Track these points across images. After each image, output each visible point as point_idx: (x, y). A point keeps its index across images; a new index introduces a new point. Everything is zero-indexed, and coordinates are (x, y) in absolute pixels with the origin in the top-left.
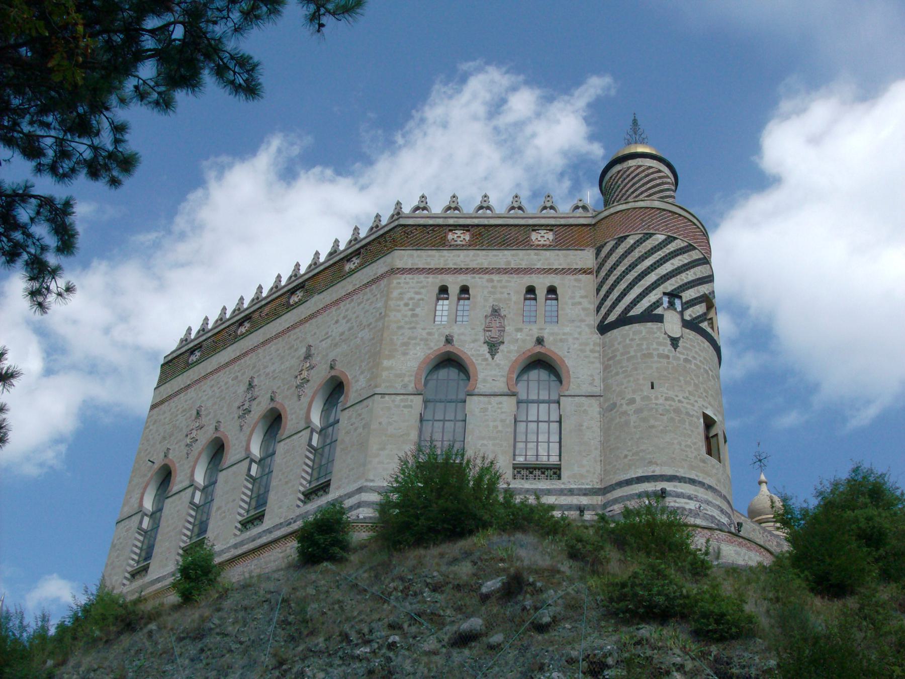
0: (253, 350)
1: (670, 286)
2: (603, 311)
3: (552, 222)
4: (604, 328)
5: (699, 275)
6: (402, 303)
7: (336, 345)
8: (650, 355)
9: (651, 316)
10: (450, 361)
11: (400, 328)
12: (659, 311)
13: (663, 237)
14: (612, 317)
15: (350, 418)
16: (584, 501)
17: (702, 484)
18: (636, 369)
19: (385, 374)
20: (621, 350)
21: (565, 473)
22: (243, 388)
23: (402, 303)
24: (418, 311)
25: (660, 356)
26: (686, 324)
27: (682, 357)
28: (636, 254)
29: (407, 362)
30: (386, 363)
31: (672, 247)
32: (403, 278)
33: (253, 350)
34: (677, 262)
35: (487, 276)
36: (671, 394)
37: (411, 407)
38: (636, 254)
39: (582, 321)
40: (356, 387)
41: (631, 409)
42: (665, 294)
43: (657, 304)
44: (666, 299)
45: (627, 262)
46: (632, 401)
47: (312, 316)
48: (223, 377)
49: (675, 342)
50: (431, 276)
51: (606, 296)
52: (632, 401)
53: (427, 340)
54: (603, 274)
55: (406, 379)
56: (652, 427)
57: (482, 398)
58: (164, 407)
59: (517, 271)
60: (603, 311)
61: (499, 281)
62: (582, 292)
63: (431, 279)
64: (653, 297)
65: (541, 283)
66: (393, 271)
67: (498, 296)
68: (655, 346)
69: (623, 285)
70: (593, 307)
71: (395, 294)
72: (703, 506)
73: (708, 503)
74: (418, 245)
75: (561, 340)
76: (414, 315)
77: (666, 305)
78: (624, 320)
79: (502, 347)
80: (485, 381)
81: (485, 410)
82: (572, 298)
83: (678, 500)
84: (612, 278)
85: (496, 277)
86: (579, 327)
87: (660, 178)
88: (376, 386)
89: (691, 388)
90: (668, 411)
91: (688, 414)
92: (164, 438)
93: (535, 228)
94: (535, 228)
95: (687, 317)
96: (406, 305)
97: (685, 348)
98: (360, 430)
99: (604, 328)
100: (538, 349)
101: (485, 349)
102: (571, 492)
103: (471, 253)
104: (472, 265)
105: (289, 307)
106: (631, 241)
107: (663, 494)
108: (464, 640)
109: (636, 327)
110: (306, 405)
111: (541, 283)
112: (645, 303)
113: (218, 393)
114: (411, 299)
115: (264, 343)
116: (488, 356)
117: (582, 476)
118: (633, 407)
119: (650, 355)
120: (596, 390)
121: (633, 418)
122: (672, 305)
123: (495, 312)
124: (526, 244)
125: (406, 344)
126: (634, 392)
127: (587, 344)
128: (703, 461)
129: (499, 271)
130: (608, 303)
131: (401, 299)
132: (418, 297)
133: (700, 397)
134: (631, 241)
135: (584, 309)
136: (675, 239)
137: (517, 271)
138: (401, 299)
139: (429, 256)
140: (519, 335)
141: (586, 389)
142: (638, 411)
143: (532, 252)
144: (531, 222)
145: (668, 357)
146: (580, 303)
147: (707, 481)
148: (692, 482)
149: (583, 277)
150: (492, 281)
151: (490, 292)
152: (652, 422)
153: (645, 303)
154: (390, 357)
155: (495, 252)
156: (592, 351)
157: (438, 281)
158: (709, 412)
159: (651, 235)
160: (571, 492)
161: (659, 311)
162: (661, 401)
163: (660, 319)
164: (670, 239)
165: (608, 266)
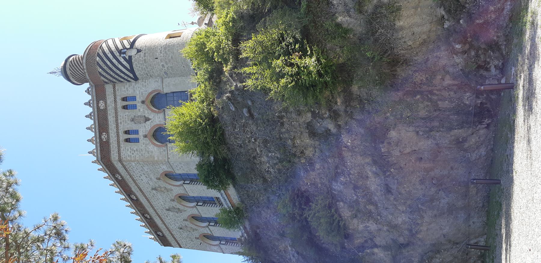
0: (155, 211)
1: (117, 54)
2: (129, 79)
3: (95, 102)
4: (136, 79)
7: (151, 179)
8: (145, 60)
9: (129, 60)
11: (142, 155)
12: (127, 57)
14: (131, 75)
15: (178, 170)
18: (150, 65)
19: (160, 158)
20: (144, 71)
22: (171, 213)
24: (135, 149)
25: (145, 57)
28: (105, 68)
29: (154, 150)
30: (156, 159)
32: (123, 156)
33: (155, 211)
36: (159, 51)
38: (105, 68)
40: (165, 168)
41: (166, 66)
43: (124, 58)
44: (122, 55)
45: (109, 71)
46: (163, 66)
47: (140, 190)
48: (167, 221)
51: (123, 78)
52: (163, 66)
54: (114, 80)
55: (162, 150)
56: (172, 57)
58: (180, 242)
59: (116, 113)
60: (129, 79)
62: (123, 88)
63: (122, 146)
64: (122, 60)
65: (120, 103)
66: (120, 160)
67: (127, 119)
69: (118, 72)
70: (128, 84)
71: (129, 158)
74: (109, 152)
75: (142, 94)
77: (125, 55)
78: (132, 70)
79: (147, 116)
80: (160, 121)
84: (116, 77)
85: (119, 121)
88: (165, 161)
90: (165, 52)
92: (192, 240)
93: (98, 108)
94: (98, 108)
95: (129, 47)
96: (133, 154)
98: (182, 165)
99: (136, 79)
101: (148, 123)
103: (110, 131)
104: (115, 130)
105: (138, 200)
108: (251, 116)
109: (134, 66)
110: (175, 187)
111: (120, 103)
112: (125, 63)
113: (172, 222)
115: (153, 208)
116: (150, 121)
118: (165, 65)
119: (145, 60)
120: (160, 80)
121: (169, 65)
122: (124, 53)
123: (133, 120)
124: (105, 110)
126: (159, 65)
127: (143, 84)
129: (117, 120)
130: (126, 77)
131: (131, 156)
132: (129, 150)
137: (116, 113)
138: (131, 156)
141: (160, 83)
142: (166, 63)
143: (108, 108)
144: (96, 110)
146: (127, 88)
149: (117, 88)
150: (121, 123)
152: (170, 58)
153: (125, 63)
154: (154, 158)
155: (109, 123)
156: (145, 82)
161: (127, 57)
162: (162, 55)
163: (130, 57)
165: (111, 79)
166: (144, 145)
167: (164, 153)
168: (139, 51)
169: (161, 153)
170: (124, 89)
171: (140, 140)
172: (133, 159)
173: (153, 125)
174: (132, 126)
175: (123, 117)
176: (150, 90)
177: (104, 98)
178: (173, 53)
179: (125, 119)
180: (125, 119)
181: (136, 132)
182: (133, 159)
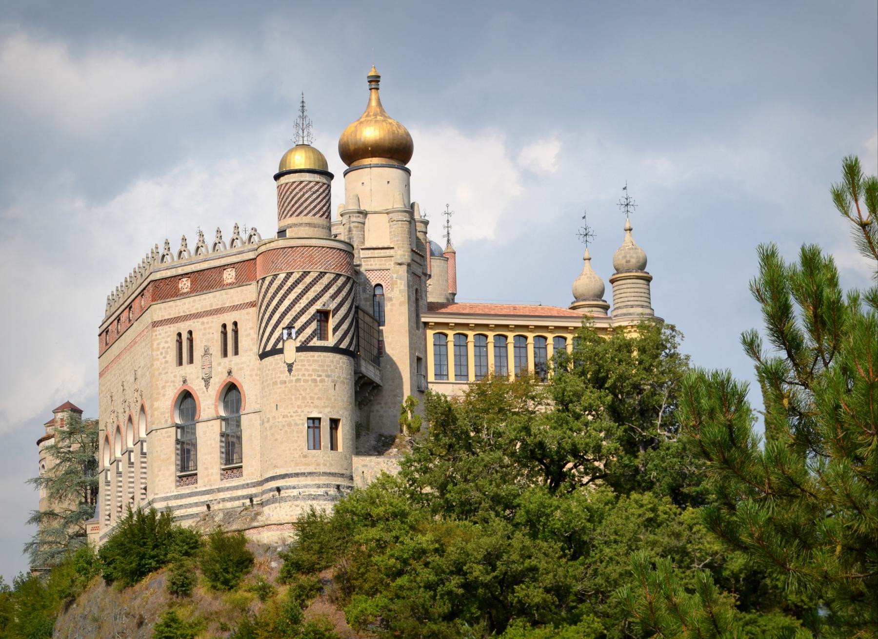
5: (302, 305)
6: (159, 353)
9: (276, 351)
10: (186, 396)
12: (280, 346)
13: (284, 275)
16: (253, 491)
17: (303, 474)
21: (245, 472)
23: (159, 353)
26: (299, 349)
30: (156, 404)
31: (289, 283)
34: (292, 296)
35: (200, 320)
36: (286, 412)
37: (169, 437)
39: (251, 350)
44: (285, 332)
47: (134, 342)
49: (290, 367)
50: (172, 325)
53: (173, 382)
61: (208, 323)
62: (250, 325)
67: (207, 336)
68: (279, 375)
70: (256, 336)
71: (155, 346)
72: (301, 490)
73: (306, 486)
75: (241, 369)
76: (166, 362)
79: (212, 381)
81: (205, 433)
83: (287, 491)
85: (205, 319)
86: (249, 356)
87: (301, 190)
89: (299, 403)
90: (284, 426)
91: (296, 424)
94: (224, 267)
95: (298, 344)
97: (297, 370)
100: (230, 380)
101: (203, 383)
102: (248, 486)
104: (193, 311)
106: (267, 282)
107: (278, 489)
111: (228, 318)
114: (164, 348)
117: (253, 474)
119: (275, 383)
121: (269, 433)
122: (290, 334)
123: (206, 352)
125: (164, 387)
128: (305, 456)
131: (158, 349)
132: (166, 345)
133: (306, 406)
134: (267, 282)
135: (252, 339)
136: (292, 273)
138: (158, 349)
139: (170, 307)
140: (220, 369)
142: (271, 428)
145: (285, 382)
148: (297, 475)
150: (203, 323)
151: (204, 334)
154: (157, 399)
156: (256, 375)
157: (175, 329)
158: (314, 415)
159: (276, 276)
160: (248, 486)
161: (280, 346)
162: (281, 419)
163: (281, 351)
164: (289, 275)
166: (173, 379)
167: (163, 421)
168: (290, 367)
169: (163, 413)
172: (154, 353)
174: (197, 354)
175: (210, 328)
177: (239, 282)
178: (281, 443)
179: (207, 334)
180: (207, 334)
181: (191, 361)
182: (154, 353)
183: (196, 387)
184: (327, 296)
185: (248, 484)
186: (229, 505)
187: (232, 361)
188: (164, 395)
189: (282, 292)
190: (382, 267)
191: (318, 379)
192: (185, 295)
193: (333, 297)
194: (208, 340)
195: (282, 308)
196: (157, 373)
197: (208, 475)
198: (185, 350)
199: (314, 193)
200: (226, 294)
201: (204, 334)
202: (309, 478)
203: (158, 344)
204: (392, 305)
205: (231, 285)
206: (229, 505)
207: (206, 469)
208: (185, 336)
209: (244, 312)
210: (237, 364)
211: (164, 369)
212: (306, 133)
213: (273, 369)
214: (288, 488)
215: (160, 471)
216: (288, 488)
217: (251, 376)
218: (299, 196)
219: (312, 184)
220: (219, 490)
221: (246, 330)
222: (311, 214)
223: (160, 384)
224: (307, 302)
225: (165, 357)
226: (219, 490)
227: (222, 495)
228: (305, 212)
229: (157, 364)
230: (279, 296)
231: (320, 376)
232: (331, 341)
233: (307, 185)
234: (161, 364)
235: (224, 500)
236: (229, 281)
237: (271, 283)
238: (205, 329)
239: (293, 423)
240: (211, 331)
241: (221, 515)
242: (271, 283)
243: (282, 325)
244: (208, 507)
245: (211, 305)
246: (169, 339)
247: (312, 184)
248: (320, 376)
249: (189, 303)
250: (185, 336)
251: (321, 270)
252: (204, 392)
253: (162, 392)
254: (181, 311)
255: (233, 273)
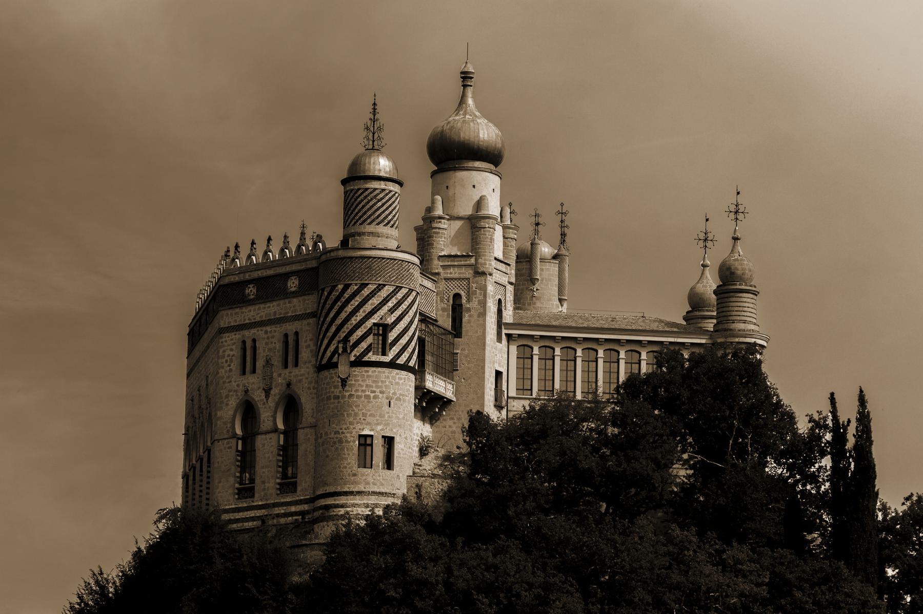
1: (342, 335)
5: (359, 318)
6: (224, 360)
12: (335, 360)
23: (224, 360)
27: (347, 394)
39: (310, 362)
42: (339, 342)
44: (341, 345)
53: (236, 391)
57: (263, 436)
64: (332, 348)
67: (270, 346)
71: (221, 353)
75: (300, 381)
76: (231, 370)
79: (272, 392)
81: (264, 445)
82: (306, 341)
85: (268, 329)
90: (335, 443)
91: (347, 442)
95: (353, 359)
101: (263, 394)
103: (257, 307)
112: (328, 354)
114: (229, 356)
123: (268, 362)
125: (227, 396)
127: (311, 382)
131: (223, 357)
132: (231, 353)
133: (358, 423)
138: (223, 357)
139: (236, 313)
142: (323, 443)
147: (356, 489)
150: (266, 332)
151: (267, 344)
153: (328, 354)
156: (314, 388)
161: (335, 360)
162: (332, 435)
167: (225, 431)
168: (344, 382)
169: (225, 423)
170: (308, 338)
171: (243, 378)
173: (260, 405)
174: (260, 363)
175: (273, 337)
176: (303, 400)
178: (332, 460)
180: (269, 343)
182: (220, 361)
183: (258, 396)
184: (385, 309)
185: (301, 500)
186: (283, 521)
187: (293, 373)
188: (227, 405)
189: (339, 304)
190: (462, 276)
191: (372, 395)
192: (251, 302)
193: (392, 311)
194: (270, 350)
195: (339, 321)
196: (221, 381)
197: (264, 489)
198: (248, 360)
199: (379, 201)
200: (290, 302)
201: (267, 344)
202: (358, 497)
203: (224, 351)
204: (470, 316)
205: (295, 294)
206: (283, 521)
207: (263, 482)
208: (249, 344)
209: (305, 322)
210: (296, 376)
211: (228, 377)
212: (376, 136)
213: (328, 384)
214: (337, 506)
215: (220, 482)
216: (337, 506)
217: (309, 388)
218: (363, 204)
219: (377, 192)
220: (275, 505)
221: (306, 341)
222: (375, 223)
223: (224, 392)
224: (364, 315)
225: (229, 366)
226: (275, 505)
227: (277, 511)
228: (369, 221)
229: (222, 371)
230: (336, 307)
231: (374, 392)
232: (387, 359)
233: (371, 193)
234: (226, 372)
235: (278, 515)
236: (293, 289)
237: (330, 294)
238: (268, 338)
239: (344, 440)
240: (274, 340)
241: (274, 531)
242: (330, 294)
243: (337, 338)
244: (263, 522)
245: (275, 313)
246: (234, 347)
247: (377, 192)
248: (374, 392)
249: (255, 310)
250: (249, 344)
251: (380, 282)
252: (264, 404)
253: (225, 401)
254: (247, 318)
255: (297, 282)
